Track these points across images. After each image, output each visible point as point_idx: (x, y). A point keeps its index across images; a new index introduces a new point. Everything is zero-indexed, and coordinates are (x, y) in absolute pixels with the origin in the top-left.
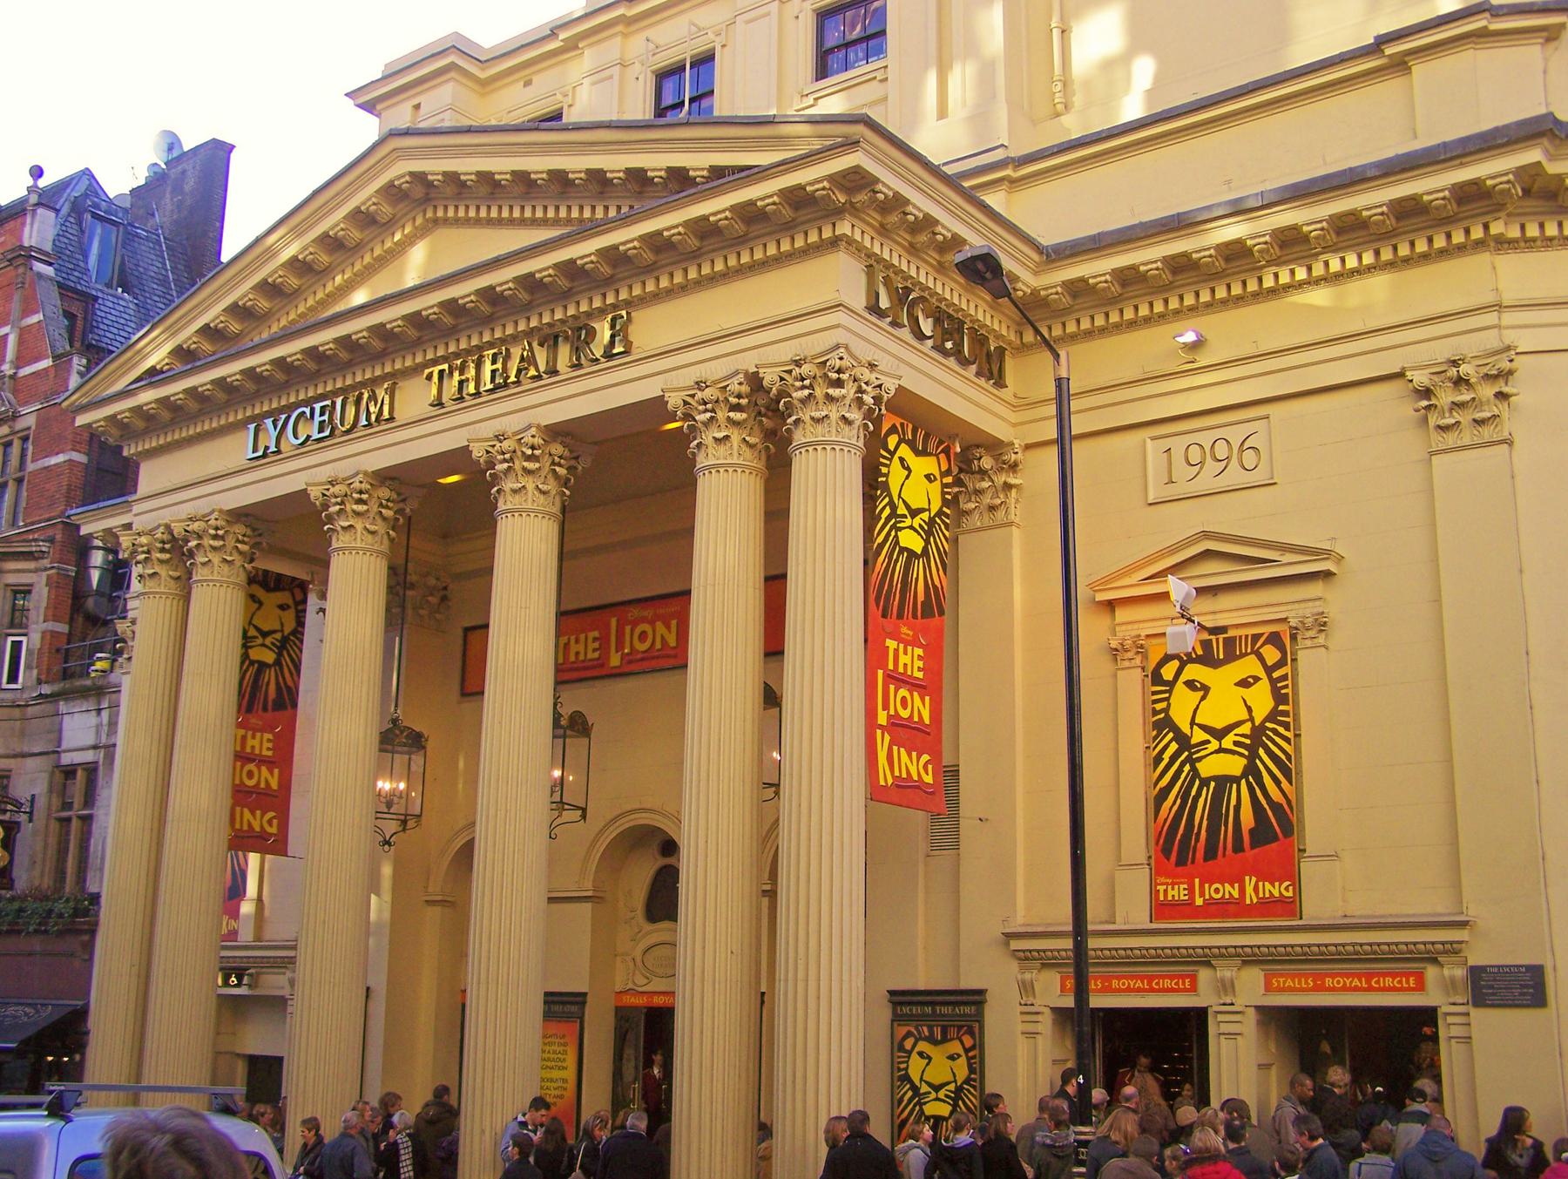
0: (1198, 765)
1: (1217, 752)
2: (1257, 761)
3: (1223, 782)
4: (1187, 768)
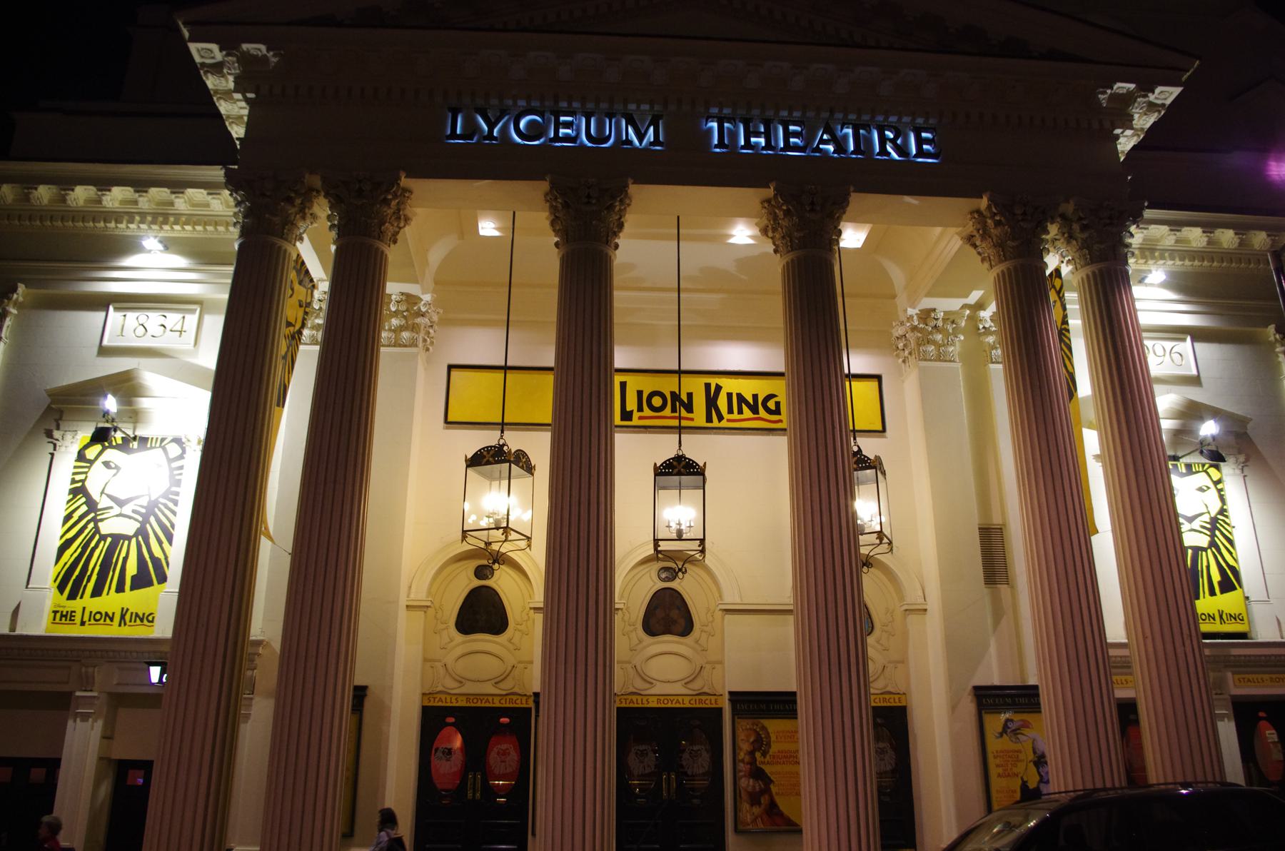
1: (117, 516)
3: (117, 539)
4: (91, 525)
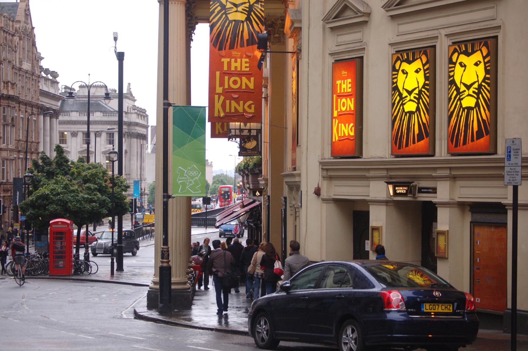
0: (228, 15)
2: (251, 16)
4: (224, 16)
